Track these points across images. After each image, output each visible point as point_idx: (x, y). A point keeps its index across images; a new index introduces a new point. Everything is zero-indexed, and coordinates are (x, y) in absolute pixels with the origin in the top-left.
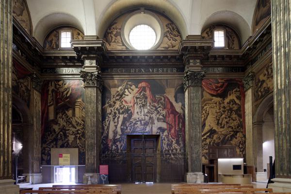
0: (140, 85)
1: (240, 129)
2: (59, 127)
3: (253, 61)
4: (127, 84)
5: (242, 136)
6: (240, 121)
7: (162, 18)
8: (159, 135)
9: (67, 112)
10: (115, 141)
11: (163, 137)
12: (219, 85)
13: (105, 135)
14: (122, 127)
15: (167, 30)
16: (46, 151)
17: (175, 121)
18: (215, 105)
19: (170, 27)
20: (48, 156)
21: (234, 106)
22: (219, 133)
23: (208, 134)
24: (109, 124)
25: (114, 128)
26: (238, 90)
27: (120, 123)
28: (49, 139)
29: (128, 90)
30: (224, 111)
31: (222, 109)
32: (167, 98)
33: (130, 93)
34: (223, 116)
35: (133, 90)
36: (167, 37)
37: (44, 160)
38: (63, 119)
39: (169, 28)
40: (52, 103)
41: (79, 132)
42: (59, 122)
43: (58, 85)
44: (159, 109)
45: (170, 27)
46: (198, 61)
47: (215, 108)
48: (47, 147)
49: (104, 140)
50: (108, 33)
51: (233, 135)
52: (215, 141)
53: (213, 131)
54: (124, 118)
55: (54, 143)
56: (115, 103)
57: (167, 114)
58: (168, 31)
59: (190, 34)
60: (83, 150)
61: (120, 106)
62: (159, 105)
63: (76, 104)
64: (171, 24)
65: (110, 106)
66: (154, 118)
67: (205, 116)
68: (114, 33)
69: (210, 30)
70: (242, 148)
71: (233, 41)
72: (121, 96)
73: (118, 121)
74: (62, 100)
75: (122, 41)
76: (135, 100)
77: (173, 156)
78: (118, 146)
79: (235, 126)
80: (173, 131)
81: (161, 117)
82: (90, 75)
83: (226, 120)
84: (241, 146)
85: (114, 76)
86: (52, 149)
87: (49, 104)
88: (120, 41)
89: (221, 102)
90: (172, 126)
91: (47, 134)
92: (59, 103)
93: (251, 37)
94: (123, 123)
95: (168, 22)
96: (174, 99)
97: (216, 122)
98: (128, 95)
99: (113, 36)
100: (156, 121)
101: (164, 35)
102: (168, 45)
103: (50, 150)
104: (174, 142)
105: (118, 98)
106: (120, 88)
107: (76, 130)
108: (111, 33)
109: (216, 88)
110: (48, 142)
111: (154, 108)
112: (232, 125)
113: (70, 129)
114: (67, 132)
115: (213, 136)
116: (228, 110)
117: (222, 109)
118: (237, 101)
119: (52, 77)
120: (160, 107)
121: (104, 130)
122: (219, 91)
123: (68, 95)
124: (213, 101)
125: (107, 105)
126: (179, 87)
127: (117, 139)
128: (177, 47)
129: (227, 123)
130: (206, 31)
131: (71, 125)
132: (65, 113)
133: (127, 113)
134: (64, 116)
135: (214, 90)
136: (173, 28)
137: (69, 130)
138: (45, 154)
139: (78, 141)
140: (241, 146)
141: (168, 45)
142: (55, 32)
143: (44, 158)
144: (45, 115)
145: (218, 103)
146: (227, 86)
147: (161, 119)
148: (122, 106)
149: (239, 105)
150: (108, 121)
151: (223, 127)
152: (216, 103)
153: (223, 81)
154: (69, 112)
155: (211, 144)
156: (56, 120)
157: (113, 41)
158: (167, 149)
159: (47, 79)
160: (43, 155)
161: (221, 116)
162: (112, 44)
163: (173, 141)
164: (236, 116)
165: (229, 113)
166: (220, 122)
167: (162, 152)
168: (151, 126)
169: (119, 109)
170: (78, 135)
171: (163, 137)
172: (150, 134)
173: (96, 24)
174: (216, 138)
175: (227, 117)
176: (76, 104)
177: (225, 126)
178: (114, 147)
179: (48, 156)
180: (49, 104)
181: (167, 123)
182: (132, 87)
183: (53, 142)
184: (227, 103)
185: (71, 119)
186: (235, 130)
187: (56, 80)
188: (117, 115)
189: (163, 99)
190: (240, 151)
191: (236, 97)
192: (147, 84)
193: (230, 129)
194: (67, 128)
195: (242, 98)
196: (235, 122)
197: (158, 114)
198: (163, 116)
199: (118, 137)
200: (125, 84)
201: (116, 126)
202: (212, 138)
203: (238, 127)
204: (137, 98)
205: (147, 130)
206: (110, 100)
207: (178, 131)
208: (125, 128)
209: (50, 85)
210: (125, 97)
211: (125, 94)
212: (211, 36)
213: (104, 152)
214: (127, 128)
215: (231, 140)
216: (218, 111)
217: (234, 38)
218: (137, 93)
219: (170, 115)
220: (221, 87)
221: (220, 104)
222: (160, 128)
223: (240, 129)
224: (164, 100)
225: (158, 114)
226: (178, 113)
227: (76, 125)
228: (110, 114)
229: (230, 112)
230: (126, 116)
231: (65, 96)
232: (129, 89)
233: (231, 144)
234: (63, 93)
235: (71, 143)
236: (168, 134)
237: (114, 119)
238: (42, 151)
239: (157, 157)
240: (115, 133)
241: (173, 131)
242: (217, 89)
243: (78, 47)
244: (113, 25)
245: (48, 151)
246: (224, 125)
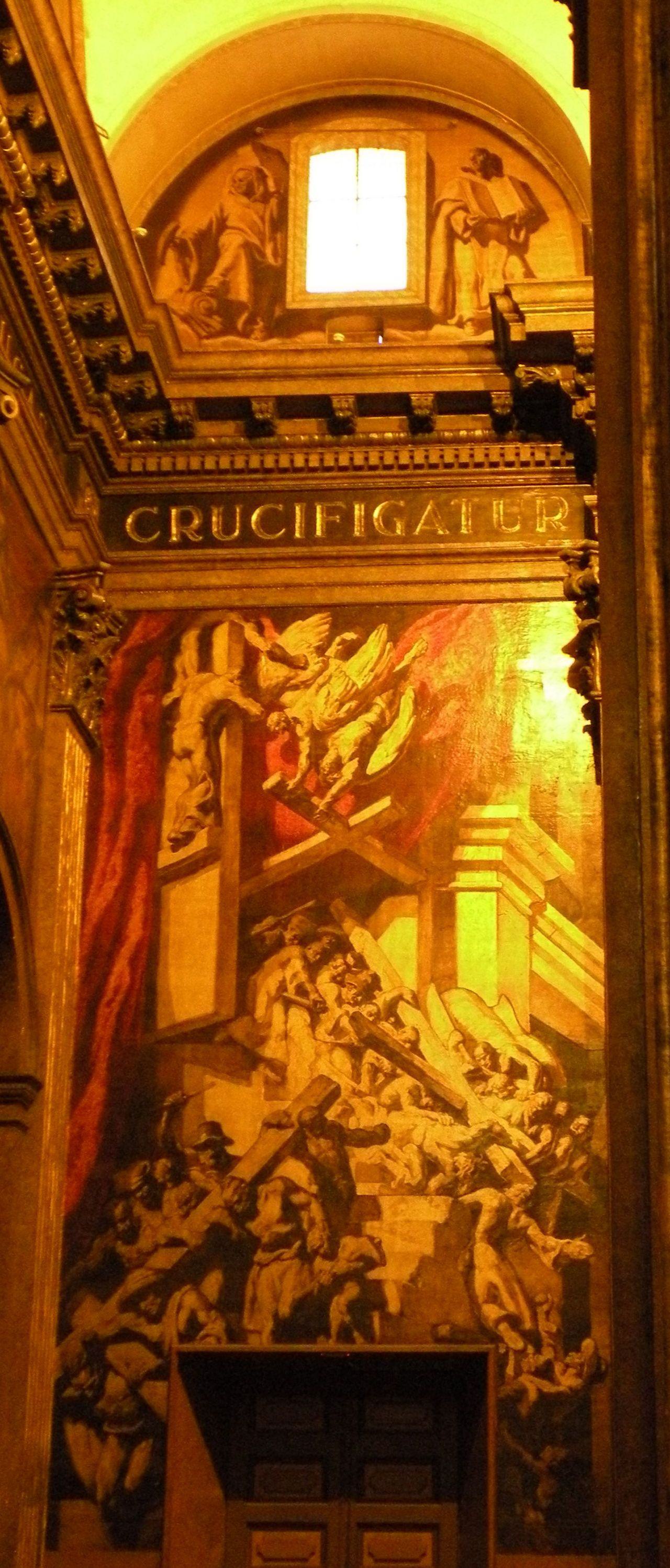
2: (267, 1109)
9: (359, 937)
16: (115, 1384)
20: (129, 1442)
28: (144, 1243)
38: (316, 1011)
40: (200, 842)
41: (501, 1157)
42: (272, 1050)
43: (278, 656)
48: (126, 1335)
55: (213, 1283)
60: (545, 1372)
63: (469, 853)
74: (309, 812)
87: (166, 858)
91: (134, 1180)
92: (279, 845)
107: (461, 1134)
113: (396, 1122)
114: (360, 1156)
119: (213, 579)
123: (380, 759)
131: (404, 1083)
132: (342, 946)
134: (325, 985)
137: (381, 1135)
138: (96, 1423)
139: (484, 1254)
142: (247, 156)
143: (82, 1467)
144: (121, 966)
154: (386, 940)
156: (238, 1030)
159: (168, 600)
160: (75, 1432)
170: (488, 1198)
176: (469, 853)
179: (129, 1442)
180: (166, 858)
183: (196, 1283)
185: (408, 1014)
187: (253, 614)
194: (362, 1120)
209: (188, 656)
227: (458, 1087)
231: (349, 771)
234: (320, 738)
235: (408, 1290)
238: (61, 1384)
245: (134, 1387)
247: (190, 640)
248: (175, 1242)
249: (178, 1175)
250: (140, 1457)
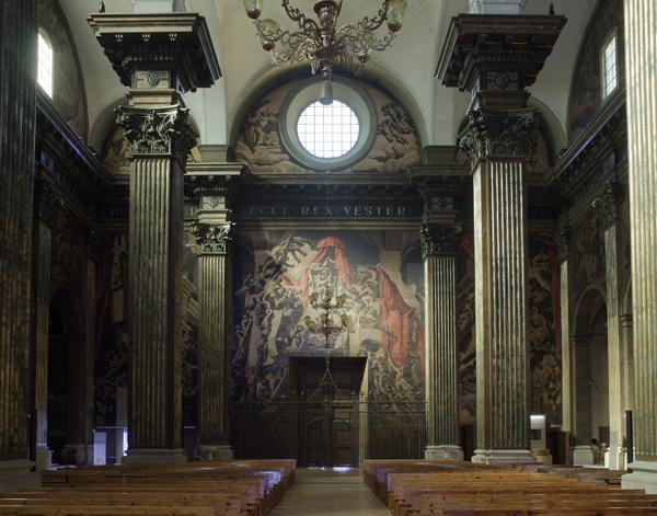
0: (322, 243)
3: (569, 204)
4: (292, 240)
7: (373, 92)
8: (364, 359)
10: (262, 371)
11: (374, 362)
13: (239, 356)
14: (280, 339)
15: (384, 118)
17: (402, 327)
19: (392, 111)
21: (536, 293)
24: (249, 332)
25: (262, 341)
26: (545, 257)
27: (275, 329)
29: (293, 254)
32: (384, 273)
33: (299, 262)
35: (305, 255)
36: (384, 133)
37: (100, 414)
39: (389, 114)
44: (364, 299)
45: (392, 111)
46: (450, 200)
49: (238, 368)
50: (250, 125)
54: (284, 319)
56: (263, 283)
57: (384, 309)
58: (387, 122)
59: (431, 144)
61: (275, 291)
62: (366, 290)
64: (393, 106)
65: (253, 290)
66: (354, 319)
68: (264, 124)
71: (536, 145)
72: (277, 269)
73: (270, 325)
75: (281, 143)
76: (310, 277)
77: (394, 407)
78: (268, 381)
80: (397, 346)
81: (370, 316)
82: (150, 118)
84: (551, 385)
85: (263, 224)
86: (118, 390)
87: (112, 287)
88: (277, 143)
90: (393, 337)
93: (565, 150)
94: (282, 329)
95: (387, 101)
96: (400, 275)
98: (293, 266)
99: (259, 130)
100: (358, 326)
101: (378, 130)
102: (386, 152)
103: (115, 392)
104: (399, 374)
105: (270, 271)
106: (276, 249)
108: (257, 124)
110: (110, 374)
111: (354, 297)
118: (543, 284)
120: (367, 293)
121: (238, 346)
125: (245, 288)
126: (409, 250)
127: (267, 366)
128: (411, 157)
133: (292, 306)
136: (398, 114)
141: (386, 152)
147: (367, 321)
148: (280, 291)
150: (246, 324)
157: (261, 141)
158: (383, 390)
160: (99, 403)
162: (258, 148)
163: (396, 373)
167: (371, 397)
168: (345, 338)
169: (273, 298)
171: (374, 362)
172: (345, 354)
173: (228, 118)
178: (259, 385)
180: (112, 287)
181: (383, 329)
182: (302, 248)
186: (538, 349)
188: (269, 311)
189: (374, 275)
190: (550, 397)
191: (541, 274)
192: (337, 241)
197: (362, 308)
198: (375, 314)
199: (270, 361)
200: (287, 240)
201: (265, 337)
203: (544, 343)
204: (314, 273)
205: (336, 347)
206: (252, 277)
207: (408, 350)
208: (286, 340)
209: (116, 242)
210: (286, 270)
211: (287, 262)
213: (236, 398)
214: (290, 341)
217: (536, 139)
218: (314, 261)
219: (392, 312)
222: (367, 343)
223: (549, 347)
224: (378, 280)
225: (362, 308)
226: (409, 308)
228: (252, 308)
230: (288, 313)
232: (297, 253)
236: (386, 355)
237: (261, 320)
238: (96, 393)
239: (361, 410)
240: (263, 352)
241: (396, 349)
243: (114, 34)
244: (262, 106)
247: (117, 237)
248: (116, 367)
249: (117, 353)
250: (111, 407)
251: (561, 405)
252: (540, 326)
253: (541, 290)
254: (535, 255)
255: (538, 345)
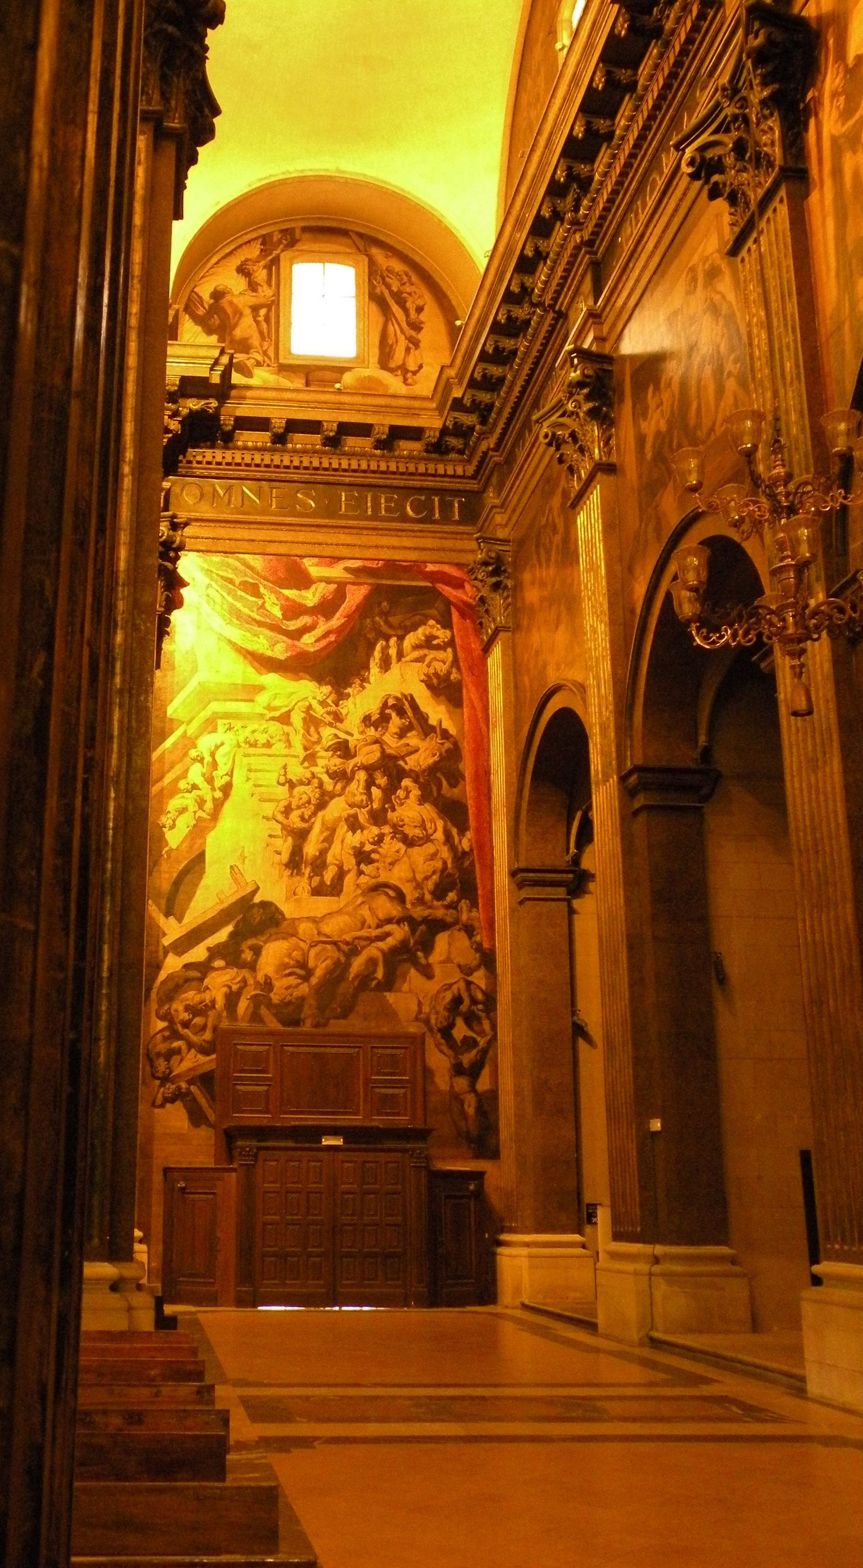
1: (453, 906)
5: (473, 958)
6: (453, 848)
12: (310, 597)
18: (275, 728)
21: (413, 739)
22: (304, 928)
23: (222, 935)
26: (443, 635)
30: (342, 777)
31: (326, 761)
34: (337, 808)
47: (279, 747)
51: (404, 943)
52: (268, 985)
53: (257, 916)
67: (201, 803)
69: (264, 252)
70: (470, 1043)
79: (418, 886)
83: (354, 839)
84: (460, 1031)
89: (319, 711)
97: (286, 846)
109: (286, 617)
112: (398, 876)
115: (257, 951)
116: (365, 768)
117: (326, 761)
122: (308, 639)
124: (262, 699)
129: (362, 857)
130: (236, 261)
135: (275, 628)
140: (460, 1031)
145: (297, 718)
146: (365, 609)
149: (445, 734)
151: (335, 889)
152: (285, 719)
153: (337, 572)
155: (243, 1005)
161: (321, 805)
164: (428, 811)
165: (376, 792)
166: (311, 849)
174: (283, 966)
175: (363, 816)
177: (349, 881)
184: (367, 720)
186: (419, 913)
190: (458, 1070)
191: (429, 686)
193: (385, 906)
195: (469, 693)
196: (418, 854)
202: (252, 967)
203: (439, 893)
212: (266, 293)
215: (389, 984)
216: (297, 771)
220: (326, 608)
221: (311, 721)
229: (382, 781)
233: (389, 1014)
242: (293, 625)
246: (341, 874)
251: (493, 1095)
252: (428, 839)
253: (427, 729)
254: (414, 628)
255: (420, 901)
